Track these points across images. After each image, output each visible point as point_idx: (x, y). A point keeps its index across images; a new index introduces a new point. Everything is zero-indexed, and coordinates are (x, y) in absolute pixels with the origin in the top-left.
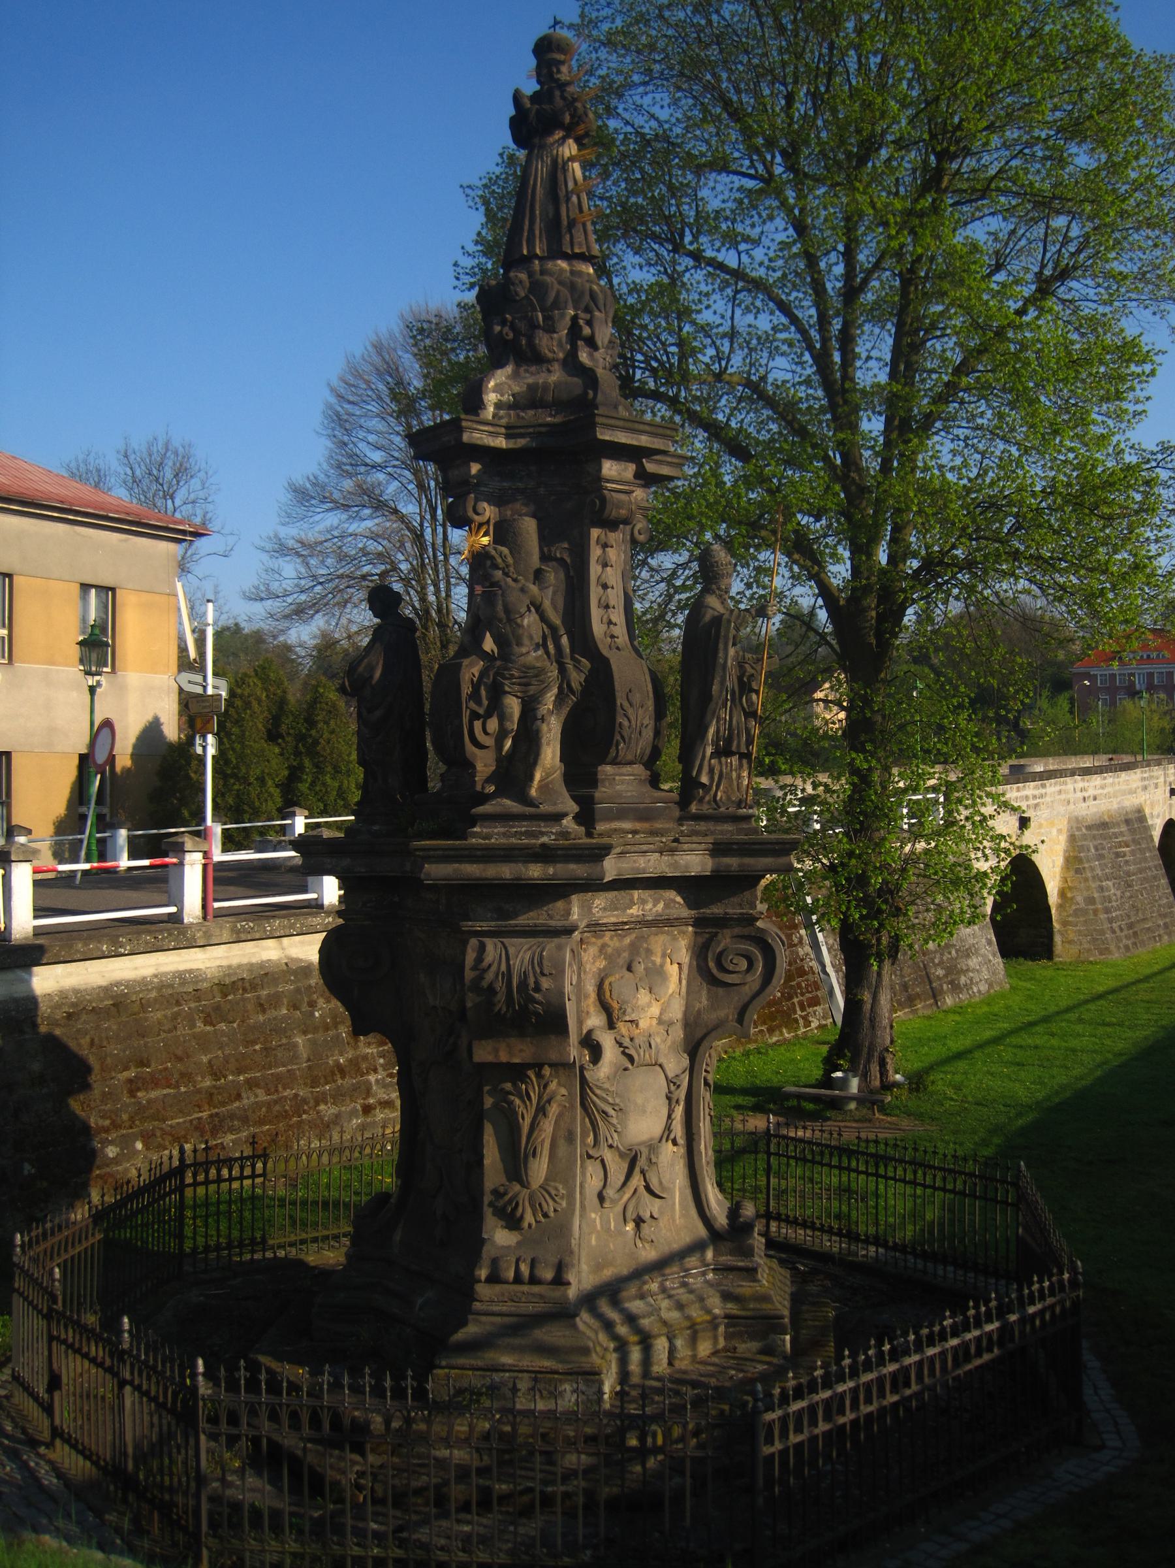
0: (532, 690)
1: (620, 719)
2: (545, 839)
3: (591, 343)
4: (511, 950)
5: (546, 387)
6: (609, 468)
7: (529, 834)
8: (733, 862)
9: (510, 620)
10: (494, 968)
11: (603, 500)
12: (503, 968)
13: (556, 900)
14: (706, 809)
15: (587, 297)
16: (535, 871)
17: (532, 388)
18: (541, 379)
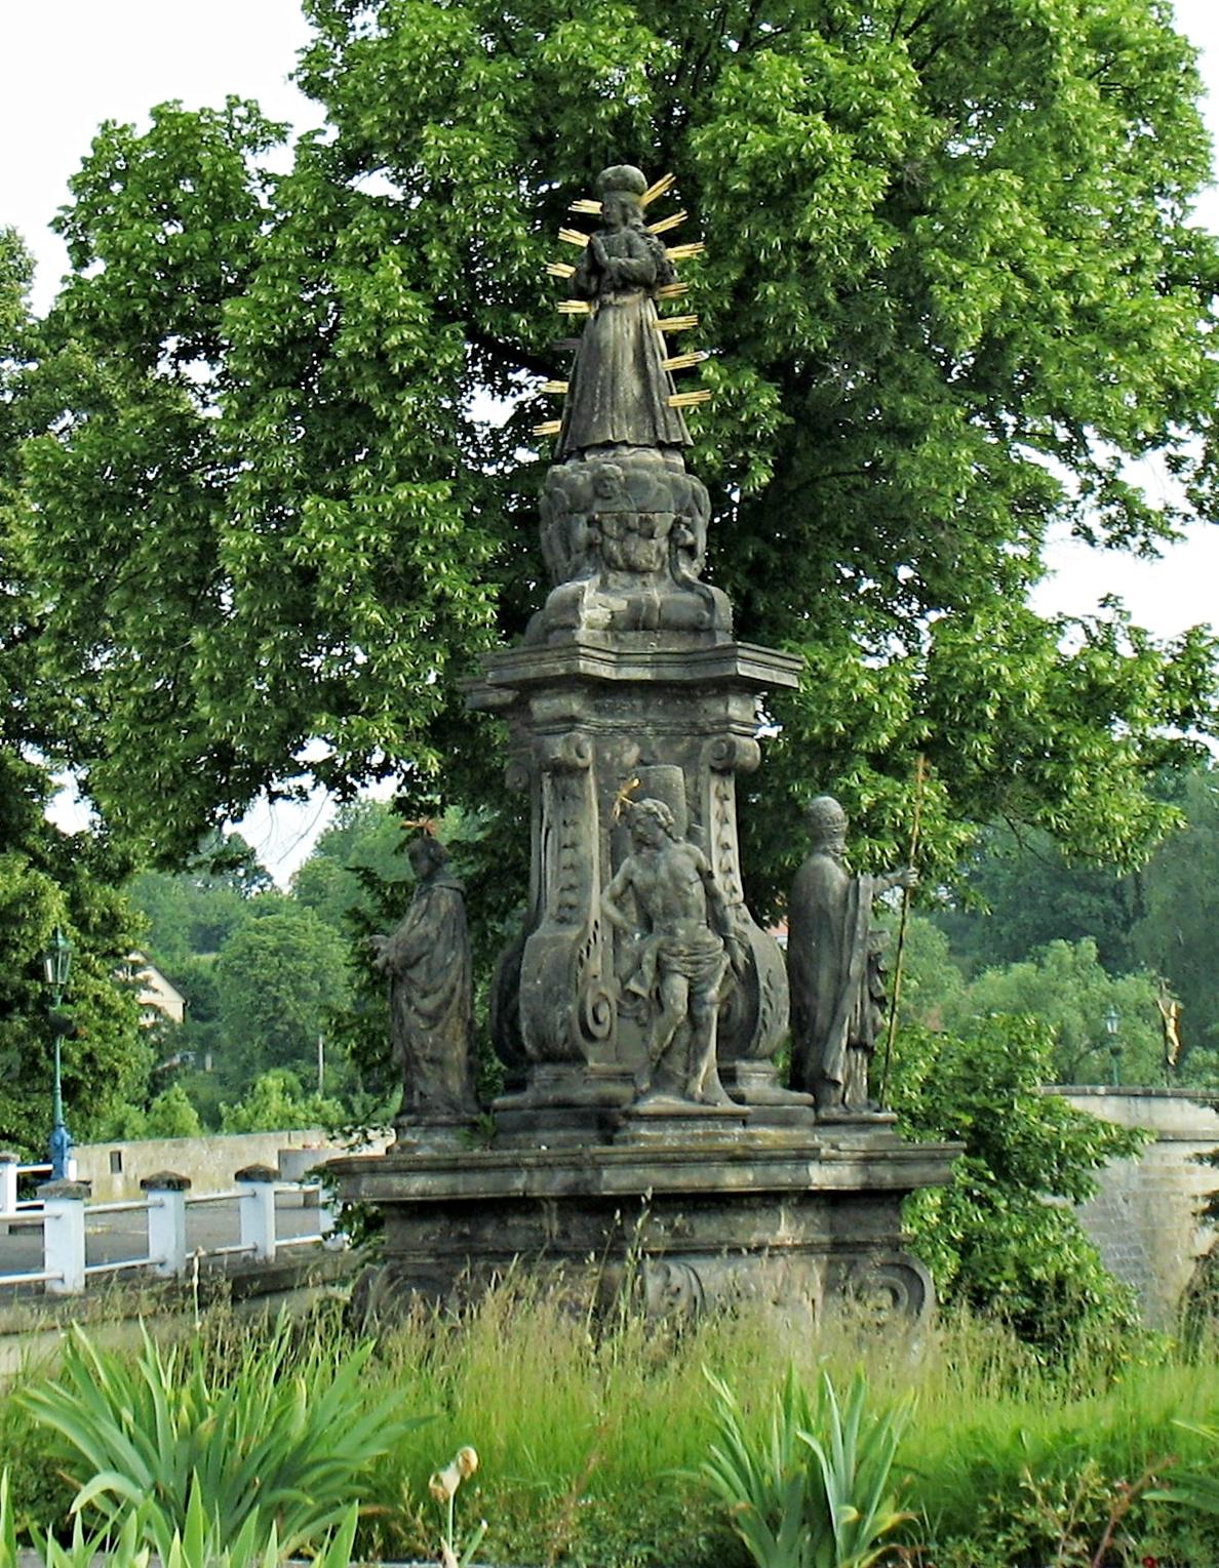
0: (705, 970)
1: (763, 1005)
2: (728, 1141)
3: (691, 550)
4: (700, 1271)
5: (651, 606)
6: (736, 708)
7: (707, 1136)
8: (886, 1175)
9: (678, 887)
10: (684, 1292)
11: (732, 746)
12: (696, 1291)
13: (737, 1214)
14: (835, 1112)
15: (690, 499)
16: (733, 1179)
17: (634, 606)
18: (638, 593)
